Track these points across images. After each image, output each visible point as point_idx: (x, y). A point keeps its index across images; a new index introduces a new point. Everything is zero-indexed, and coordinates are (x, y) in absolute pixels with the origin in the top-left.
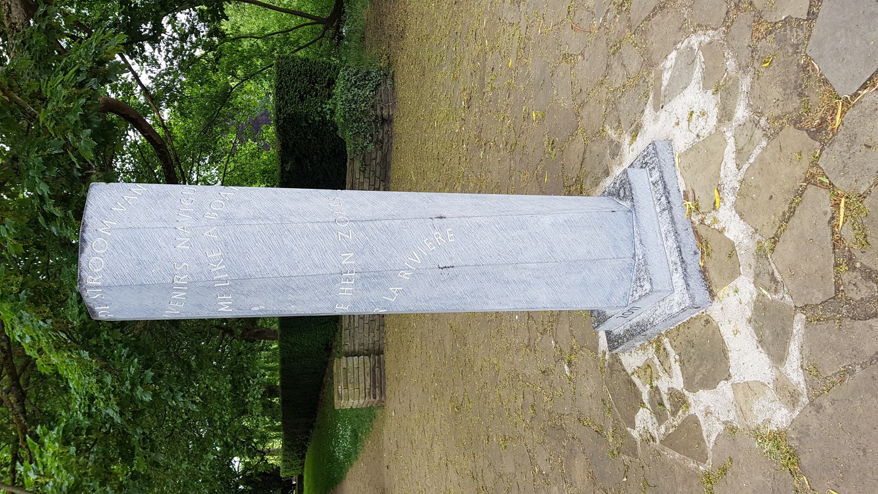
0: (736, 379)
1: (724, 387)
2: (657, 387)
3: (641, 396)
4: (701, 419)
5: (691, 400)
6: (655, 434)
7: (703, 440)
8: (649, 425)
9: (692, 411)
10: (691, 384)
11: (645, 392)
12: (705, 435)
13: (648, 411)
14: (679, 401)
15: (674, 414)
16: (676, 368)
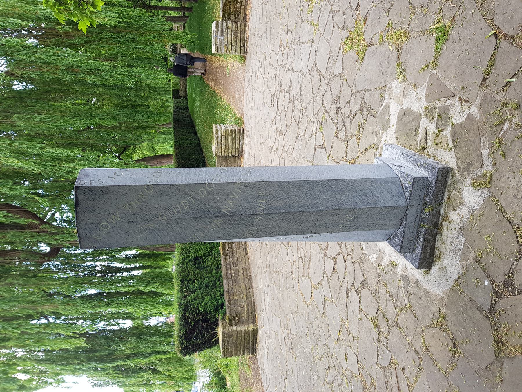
0: (400, 107)
1: (405, 107)
2: (436, 128)
3: (451, 131)
4: (424, 98)
5: (423, 110)
6: (457, 102)
7: (428, 87)
8: (459, 110)
9: (426, 104)
10: (418, 117)
11: (447, 133)
12: (426, 89)
13: (453, 119)
14: (429, 112)
15: (435, 108)
16: (421, 130)
